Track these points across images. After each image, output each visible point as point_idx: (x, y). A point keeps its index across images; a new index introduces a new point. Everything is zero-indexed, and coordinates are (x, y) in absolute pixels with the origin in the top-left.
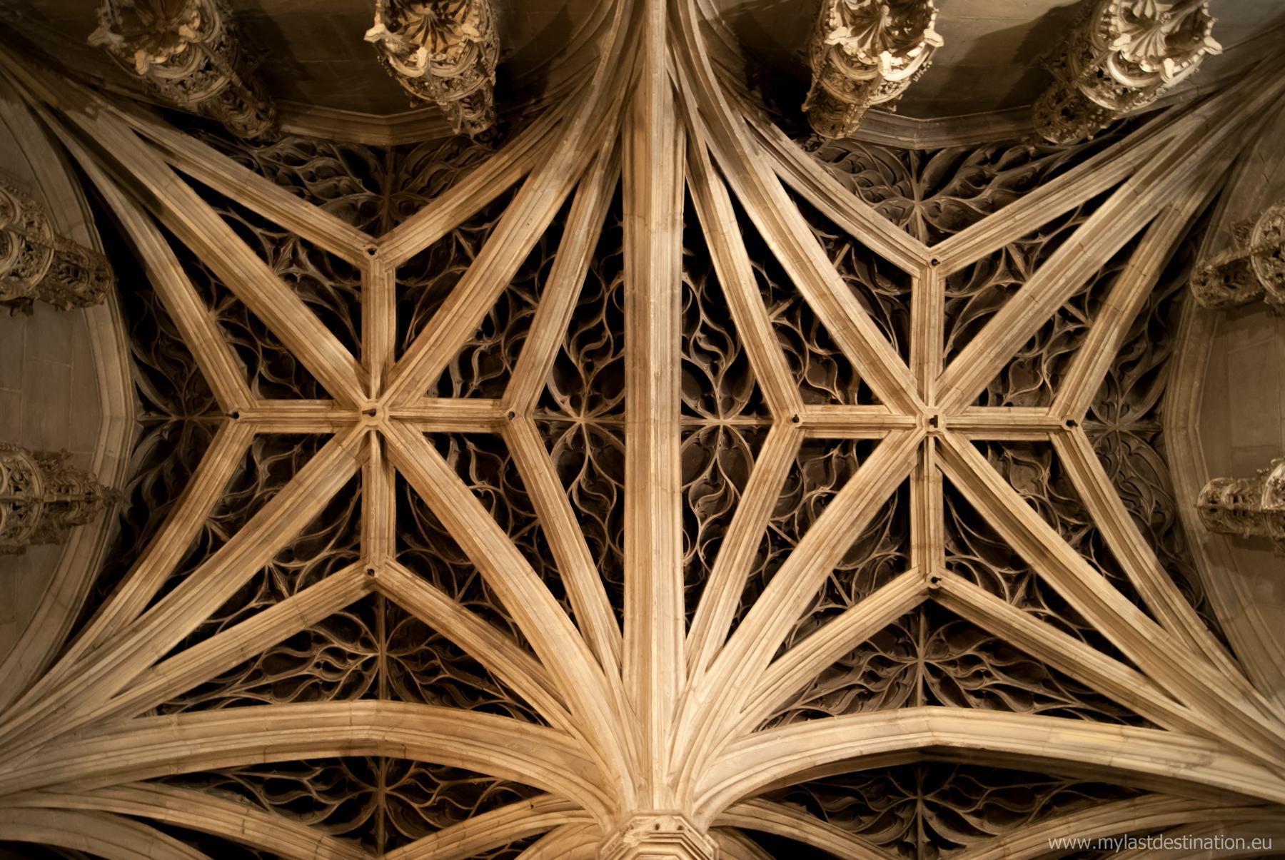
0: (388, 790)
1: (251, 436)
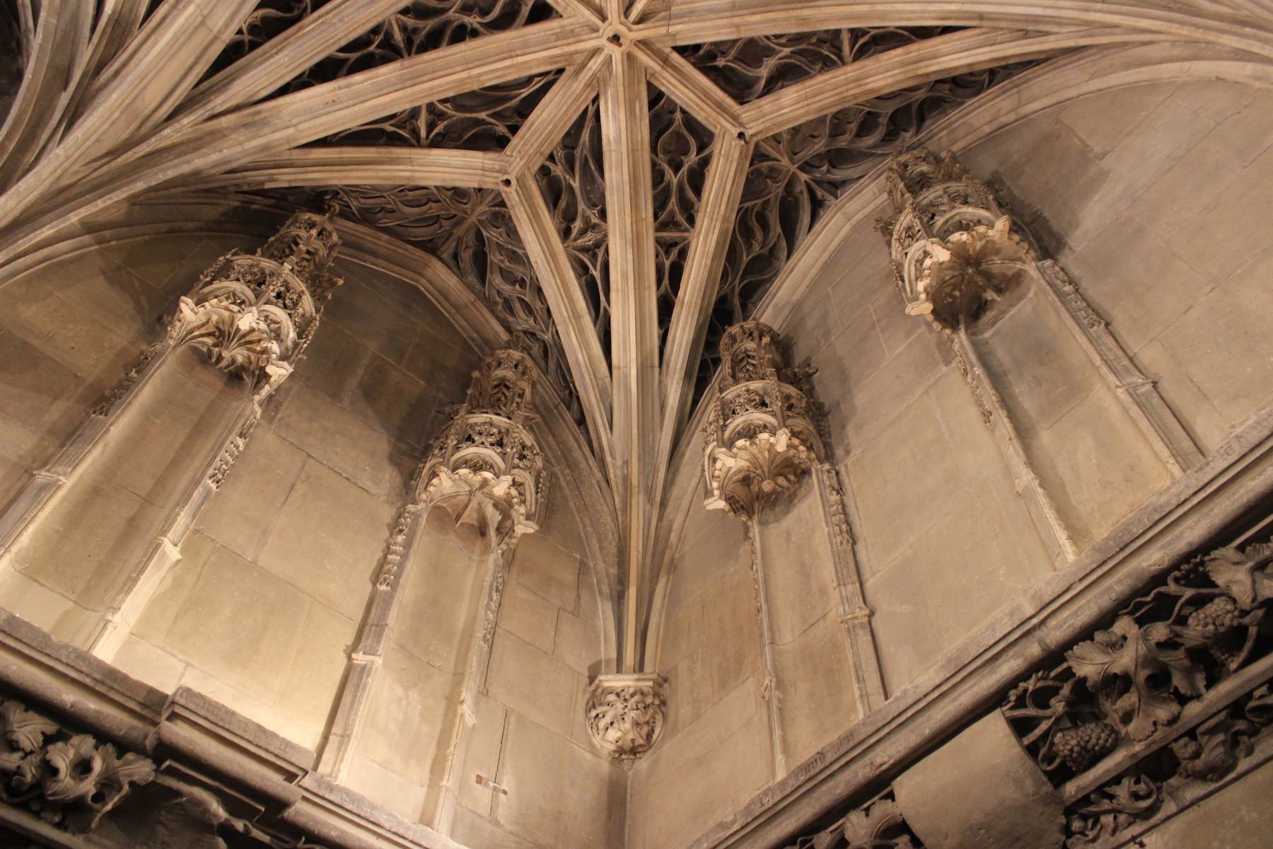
1: (746, 107)
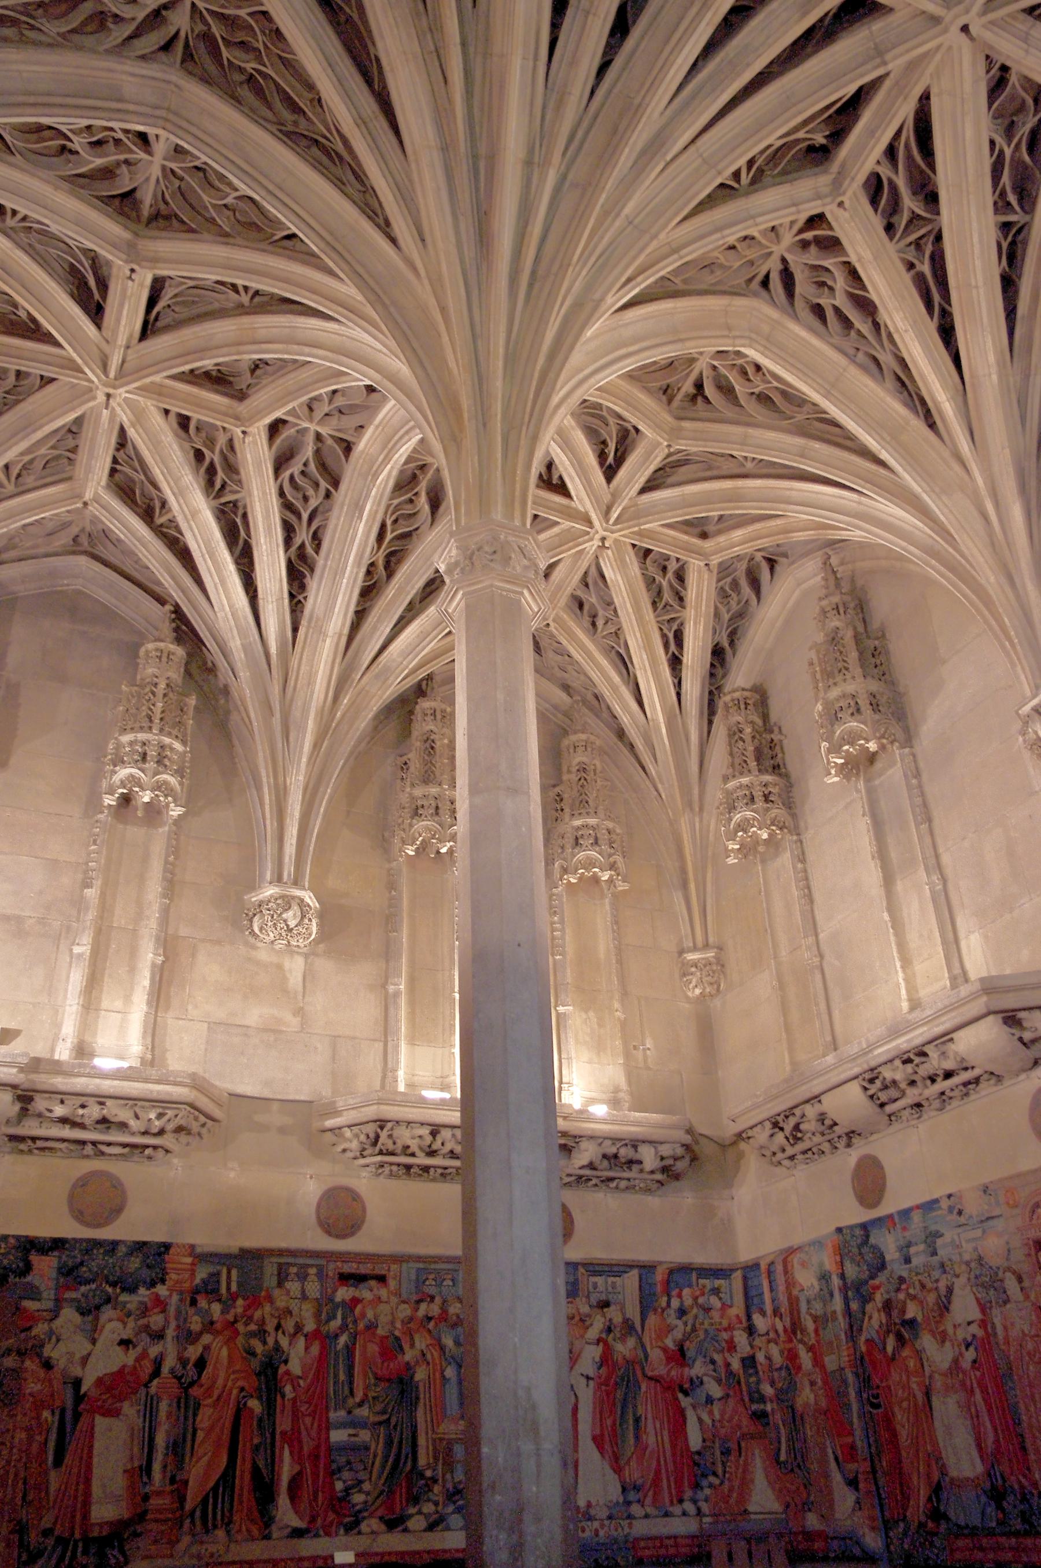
0: (774, 248)
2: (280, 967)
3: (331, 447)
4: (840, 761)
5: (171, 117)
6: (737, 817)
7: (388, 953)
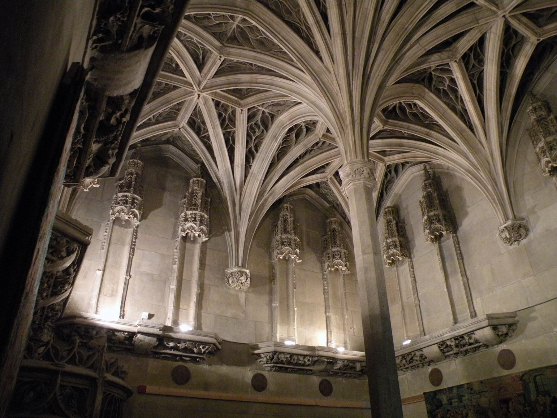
2: (237, 296)
3: (267, 116)
4: (433, 237)
5: (250, 13)
6: (391, 252)
7: (271, 293)
